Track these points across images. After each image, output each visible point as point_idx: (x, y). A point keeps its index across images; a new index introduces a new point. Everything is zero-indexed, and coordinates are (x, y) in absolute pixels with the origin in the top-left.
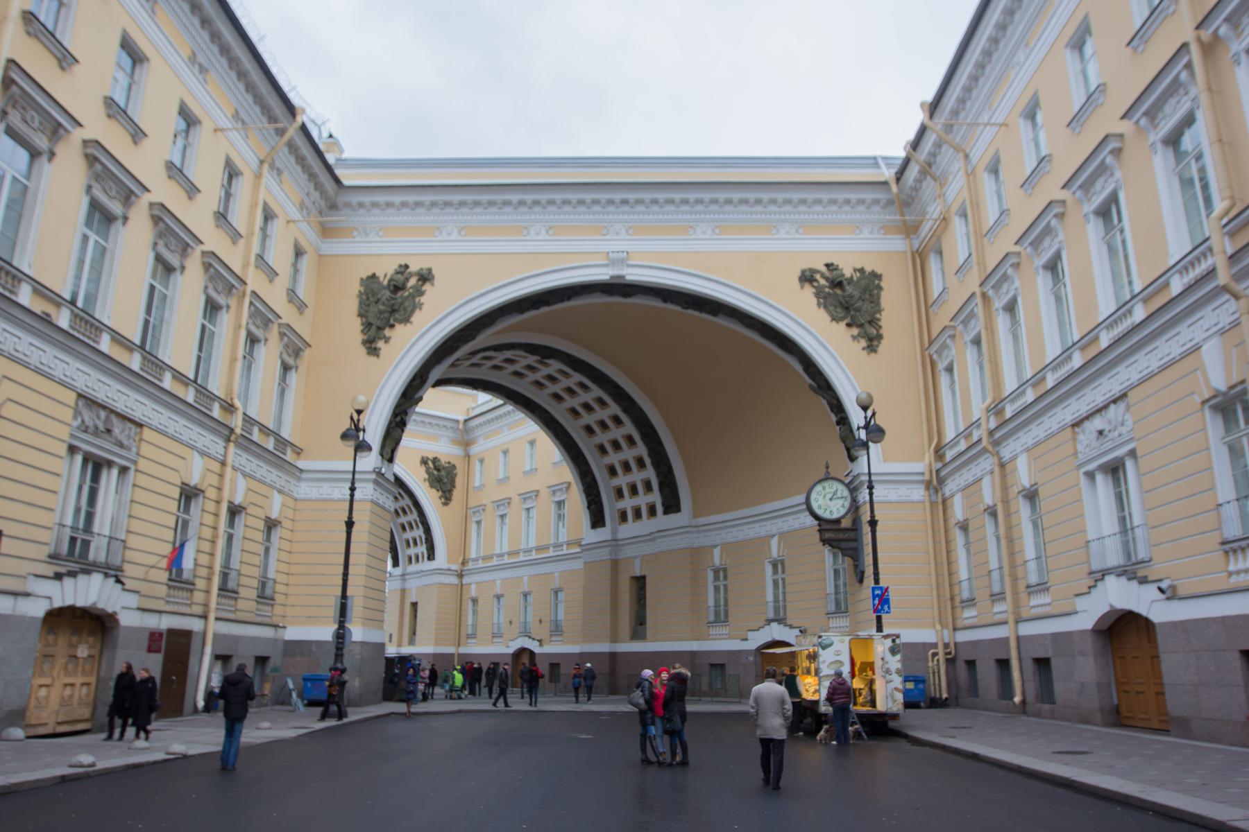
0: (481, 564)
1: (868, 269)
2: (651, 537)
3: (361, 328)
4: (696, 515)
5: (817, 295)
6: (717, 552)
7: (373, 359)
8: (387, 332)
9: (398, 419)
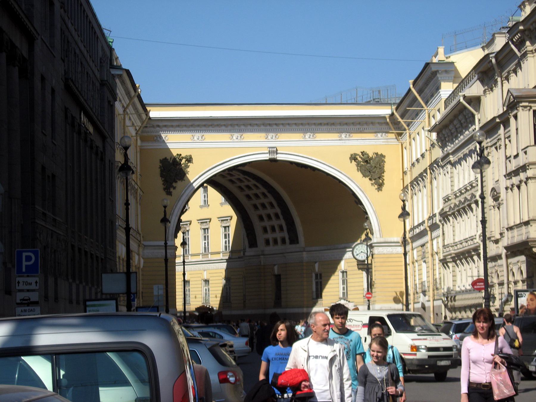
1: (379, 153)
3: (162, 182)
7: (169, 197)
8: (174, 184)
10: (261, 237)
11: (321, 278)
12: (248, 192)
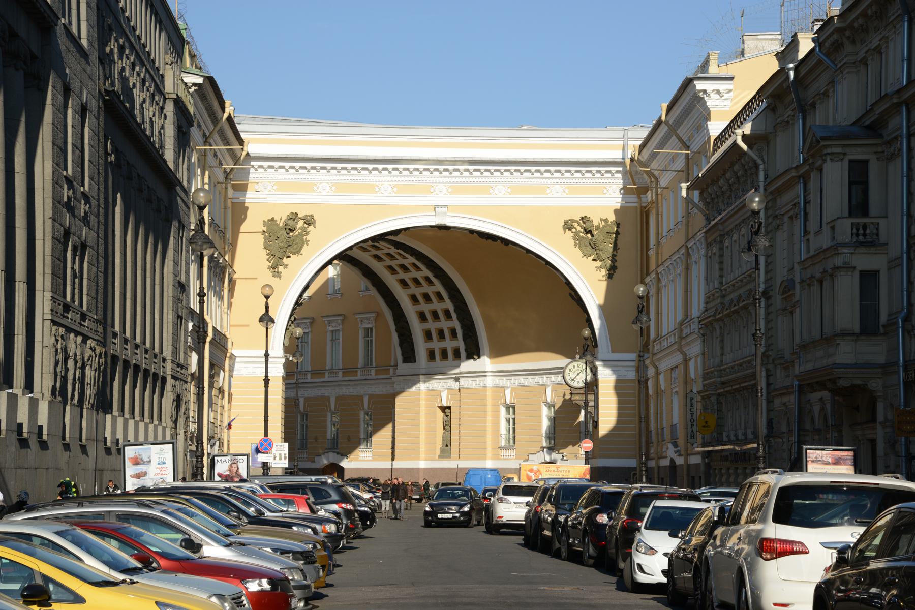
5: (574, 238)
8: (285, 261)
10: (421, 347)
12: (402, 275)
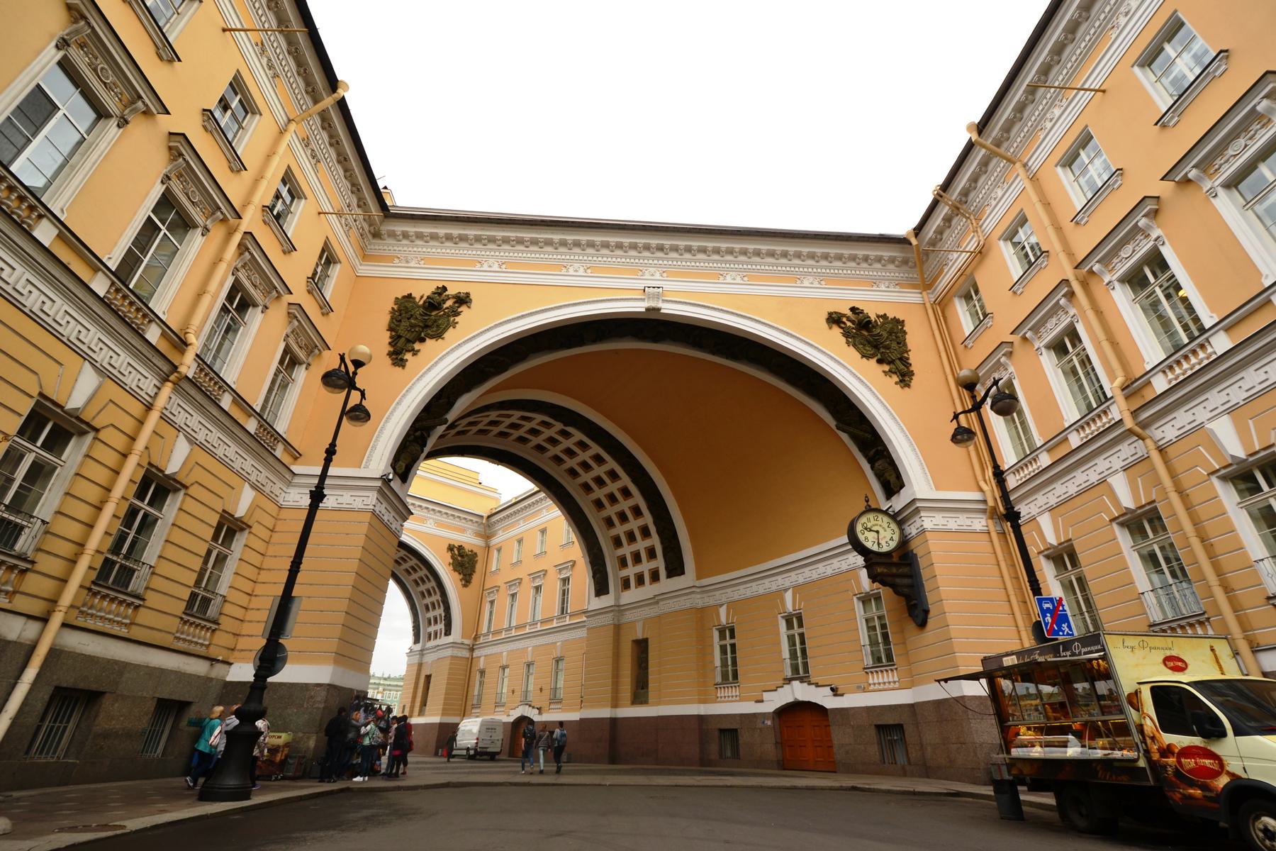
0: (491, 638)
1: (891, 316)
2: (655, 600)
4: (699, 577)
6: (723, 611)
7: (398, 369)
8: (417, 346)
9: (418, 433)
11: (732, 636)
